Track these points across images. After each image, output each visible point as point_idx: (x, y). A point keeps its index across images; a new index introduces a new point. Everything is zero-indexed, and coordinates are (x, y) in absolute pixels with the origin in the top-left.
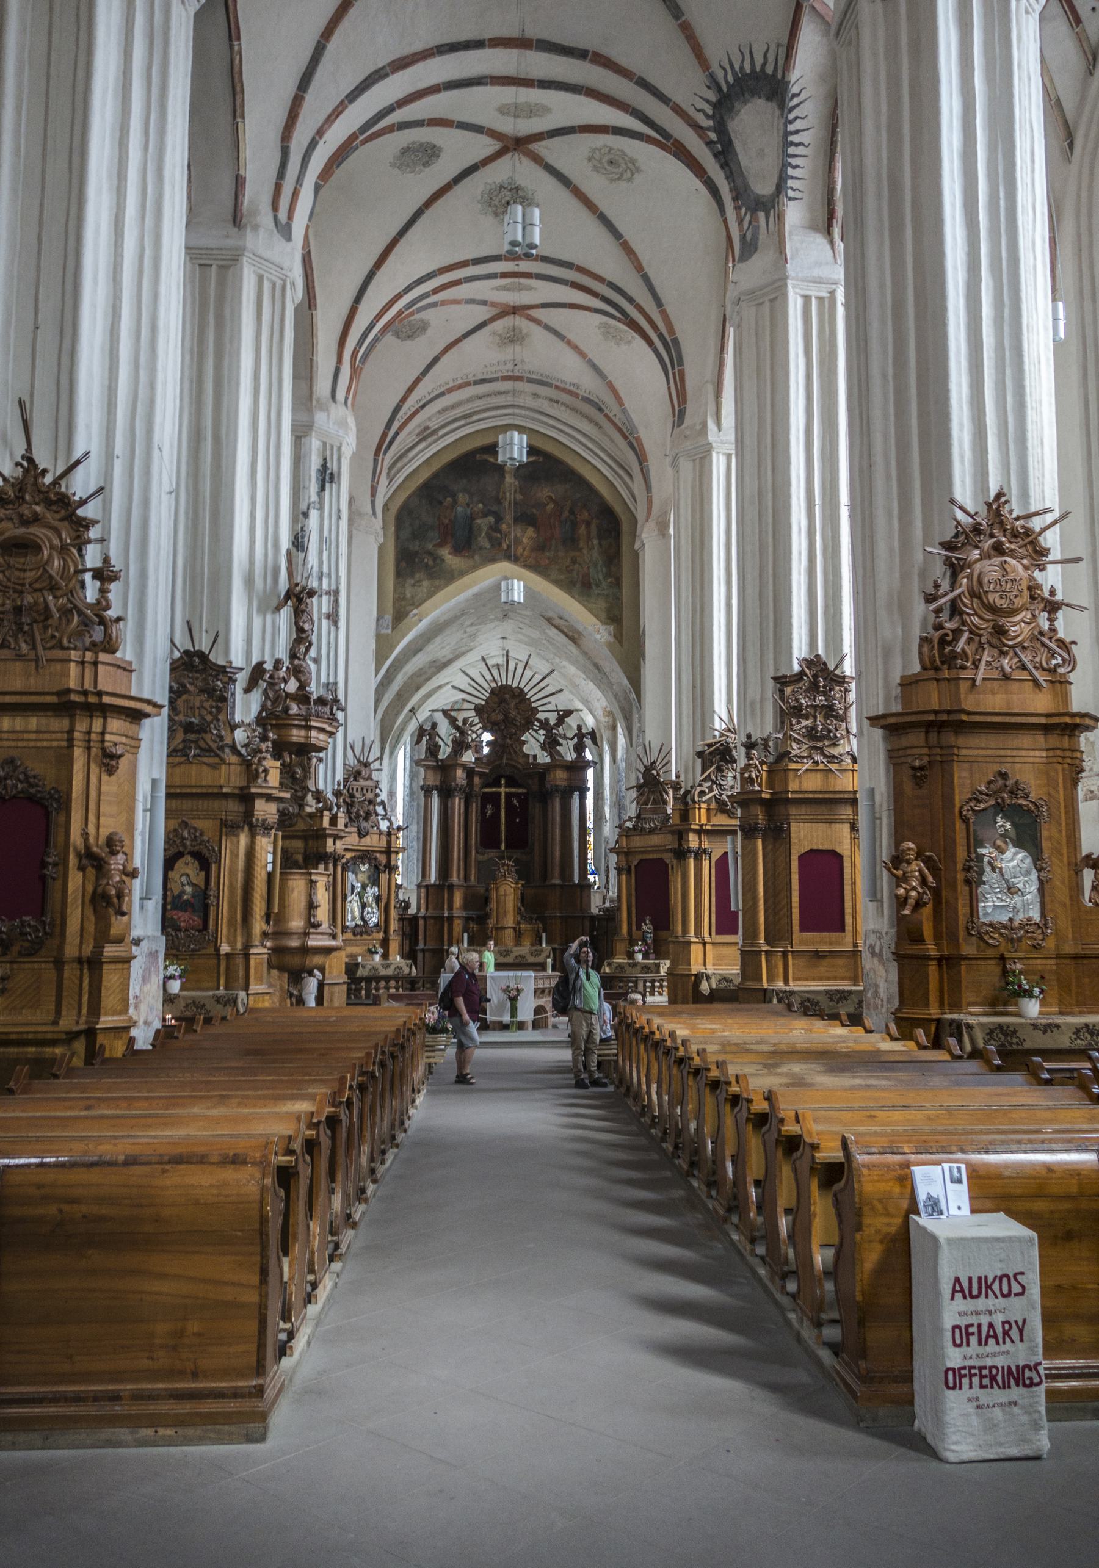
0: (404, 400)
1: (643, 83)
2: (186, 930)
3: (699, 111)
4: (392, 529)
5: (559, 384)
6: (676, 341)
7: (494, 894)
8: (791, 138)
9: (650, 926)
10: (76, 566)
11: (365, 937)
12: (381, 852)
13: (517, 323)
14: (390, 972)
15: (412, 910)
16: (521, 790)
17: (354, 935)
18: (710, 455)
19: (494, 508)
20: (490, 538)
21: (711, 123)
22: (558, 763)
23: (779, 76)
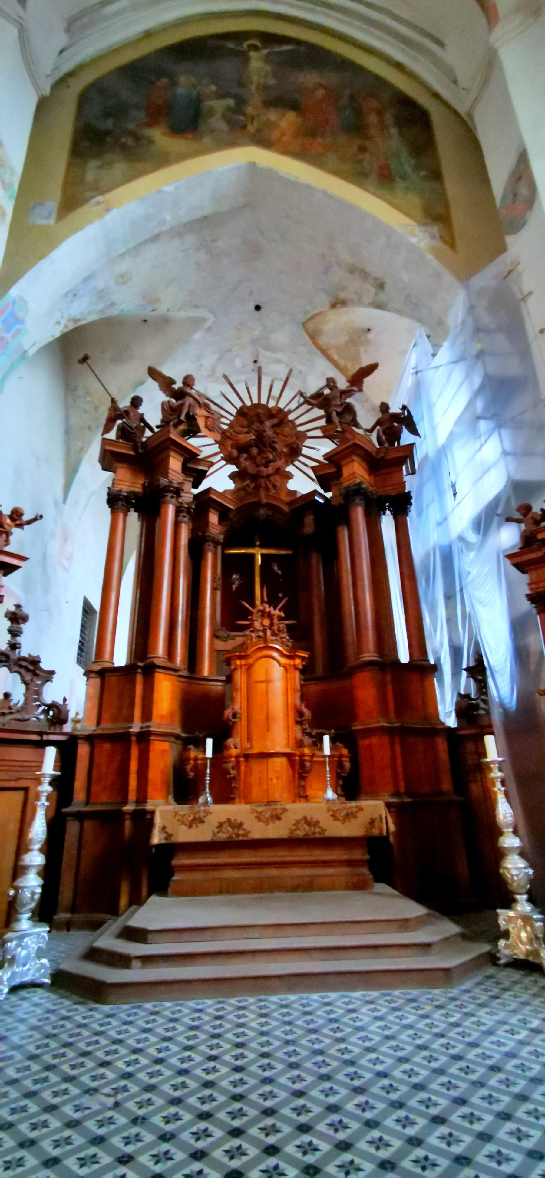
7: (240, 678)
19: (235, 90)
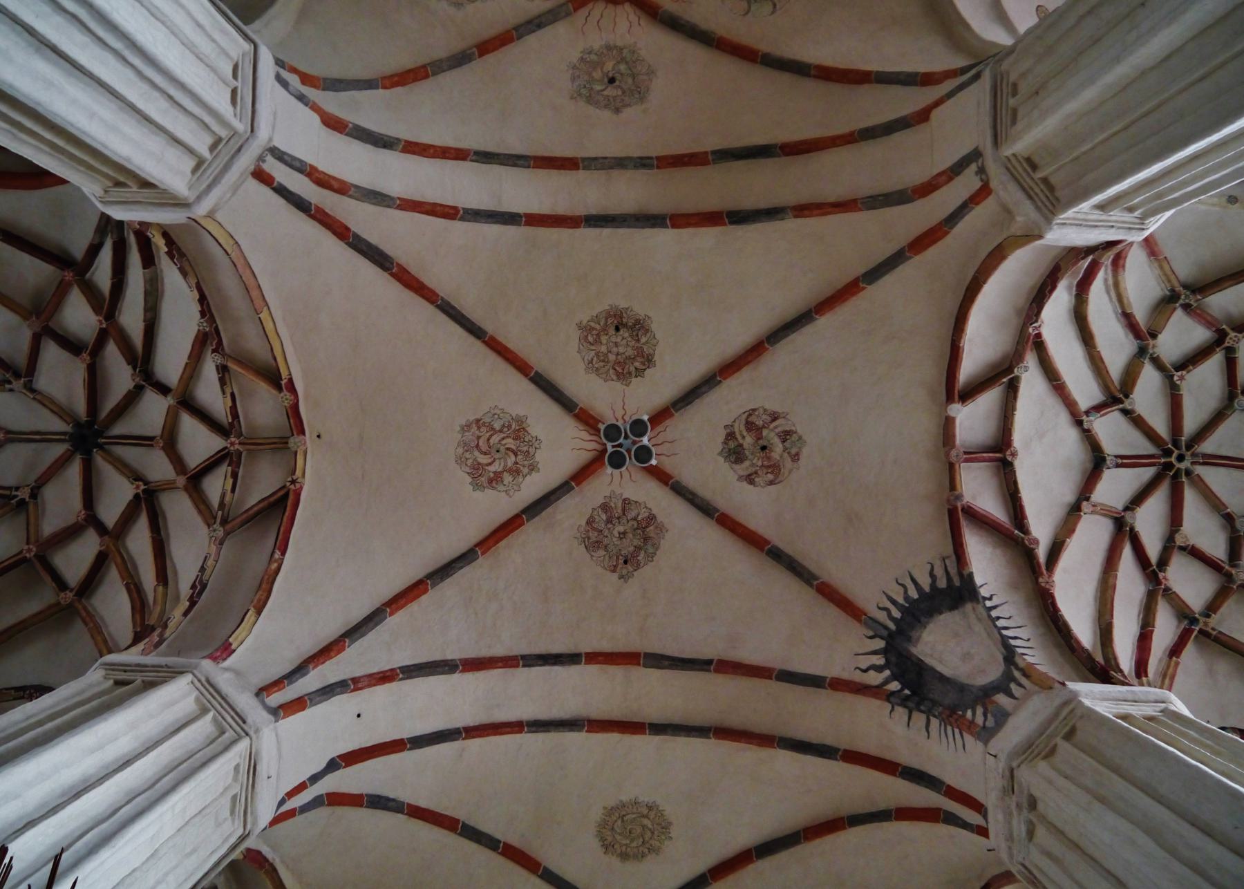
3: (865, 671)
21: (887, 673)
23: (957, 582)
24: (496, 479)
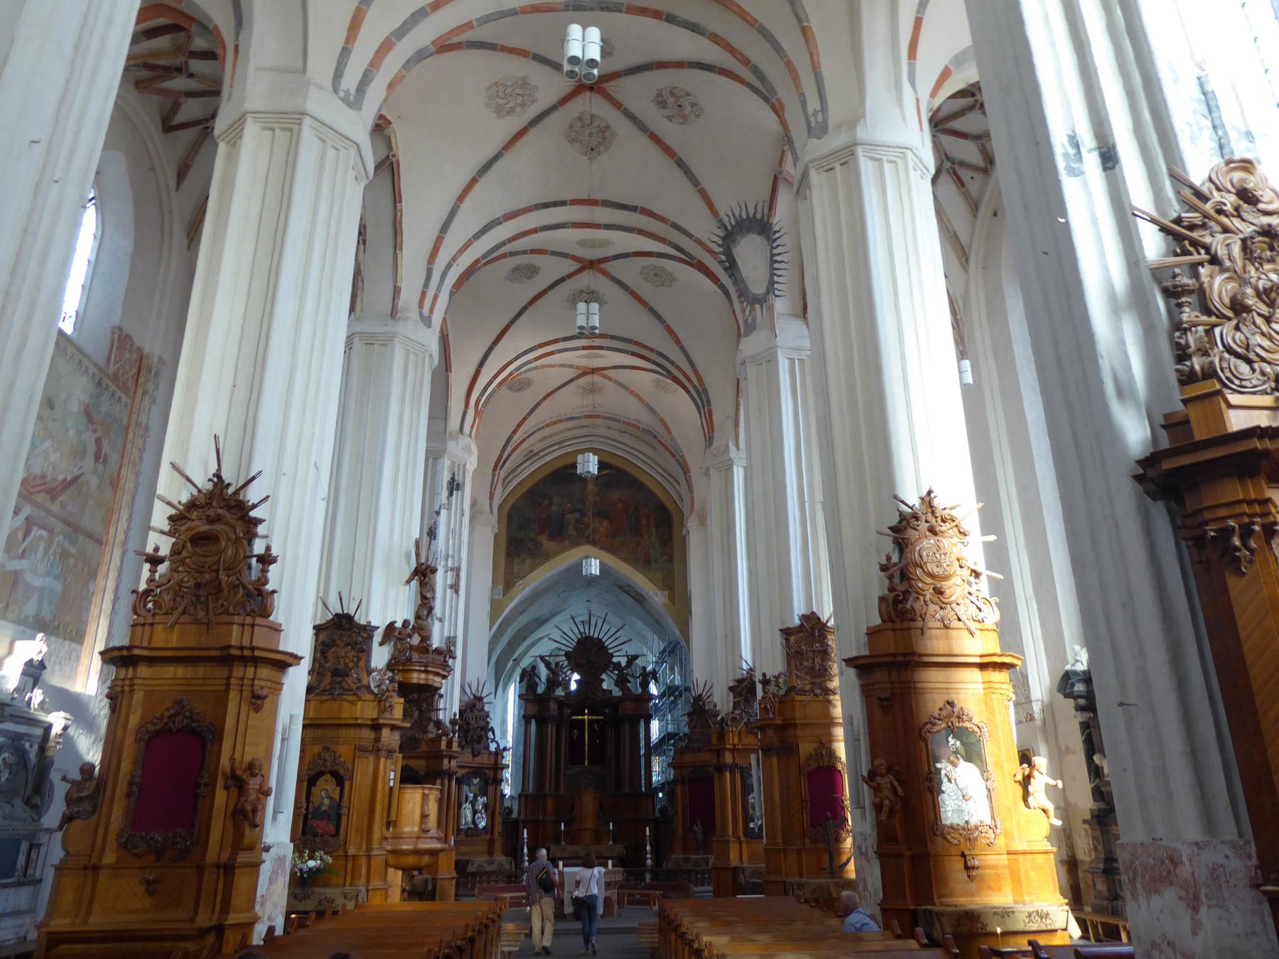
0: (515, 432)
1: (675, 226)
2: (322, 836)
4: (505, 523)
5: (625, 420)
6: (705, 391)
8: (775, 258)
9: (700, 827)
10: (245, 553)
11: (475, 838)
12: (489, 768)
13: (595, 380)
14: (493, 868)
15: (515, 815)
16: (600, 717)
17: (466, 836)
18: (732, 468)
20: (577, 529)
21: (721, 249)
22: (628, 696)
23: (766, 220)
24: (511, 111)
